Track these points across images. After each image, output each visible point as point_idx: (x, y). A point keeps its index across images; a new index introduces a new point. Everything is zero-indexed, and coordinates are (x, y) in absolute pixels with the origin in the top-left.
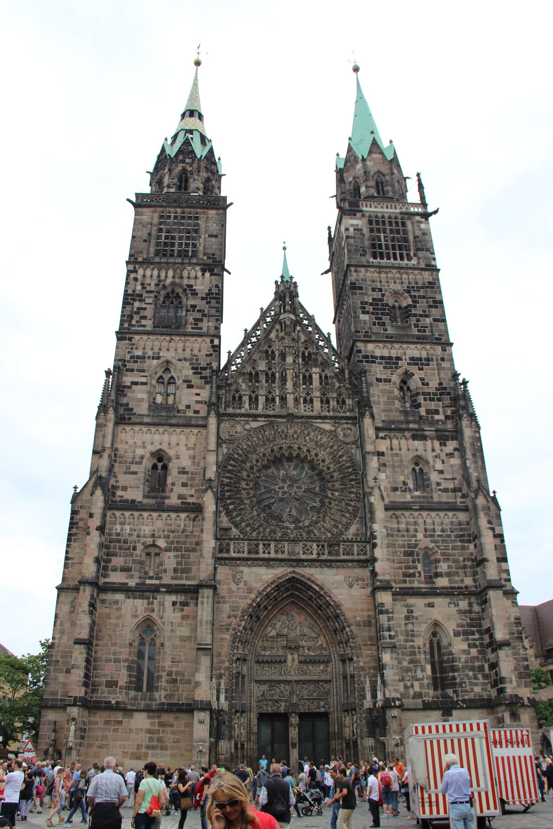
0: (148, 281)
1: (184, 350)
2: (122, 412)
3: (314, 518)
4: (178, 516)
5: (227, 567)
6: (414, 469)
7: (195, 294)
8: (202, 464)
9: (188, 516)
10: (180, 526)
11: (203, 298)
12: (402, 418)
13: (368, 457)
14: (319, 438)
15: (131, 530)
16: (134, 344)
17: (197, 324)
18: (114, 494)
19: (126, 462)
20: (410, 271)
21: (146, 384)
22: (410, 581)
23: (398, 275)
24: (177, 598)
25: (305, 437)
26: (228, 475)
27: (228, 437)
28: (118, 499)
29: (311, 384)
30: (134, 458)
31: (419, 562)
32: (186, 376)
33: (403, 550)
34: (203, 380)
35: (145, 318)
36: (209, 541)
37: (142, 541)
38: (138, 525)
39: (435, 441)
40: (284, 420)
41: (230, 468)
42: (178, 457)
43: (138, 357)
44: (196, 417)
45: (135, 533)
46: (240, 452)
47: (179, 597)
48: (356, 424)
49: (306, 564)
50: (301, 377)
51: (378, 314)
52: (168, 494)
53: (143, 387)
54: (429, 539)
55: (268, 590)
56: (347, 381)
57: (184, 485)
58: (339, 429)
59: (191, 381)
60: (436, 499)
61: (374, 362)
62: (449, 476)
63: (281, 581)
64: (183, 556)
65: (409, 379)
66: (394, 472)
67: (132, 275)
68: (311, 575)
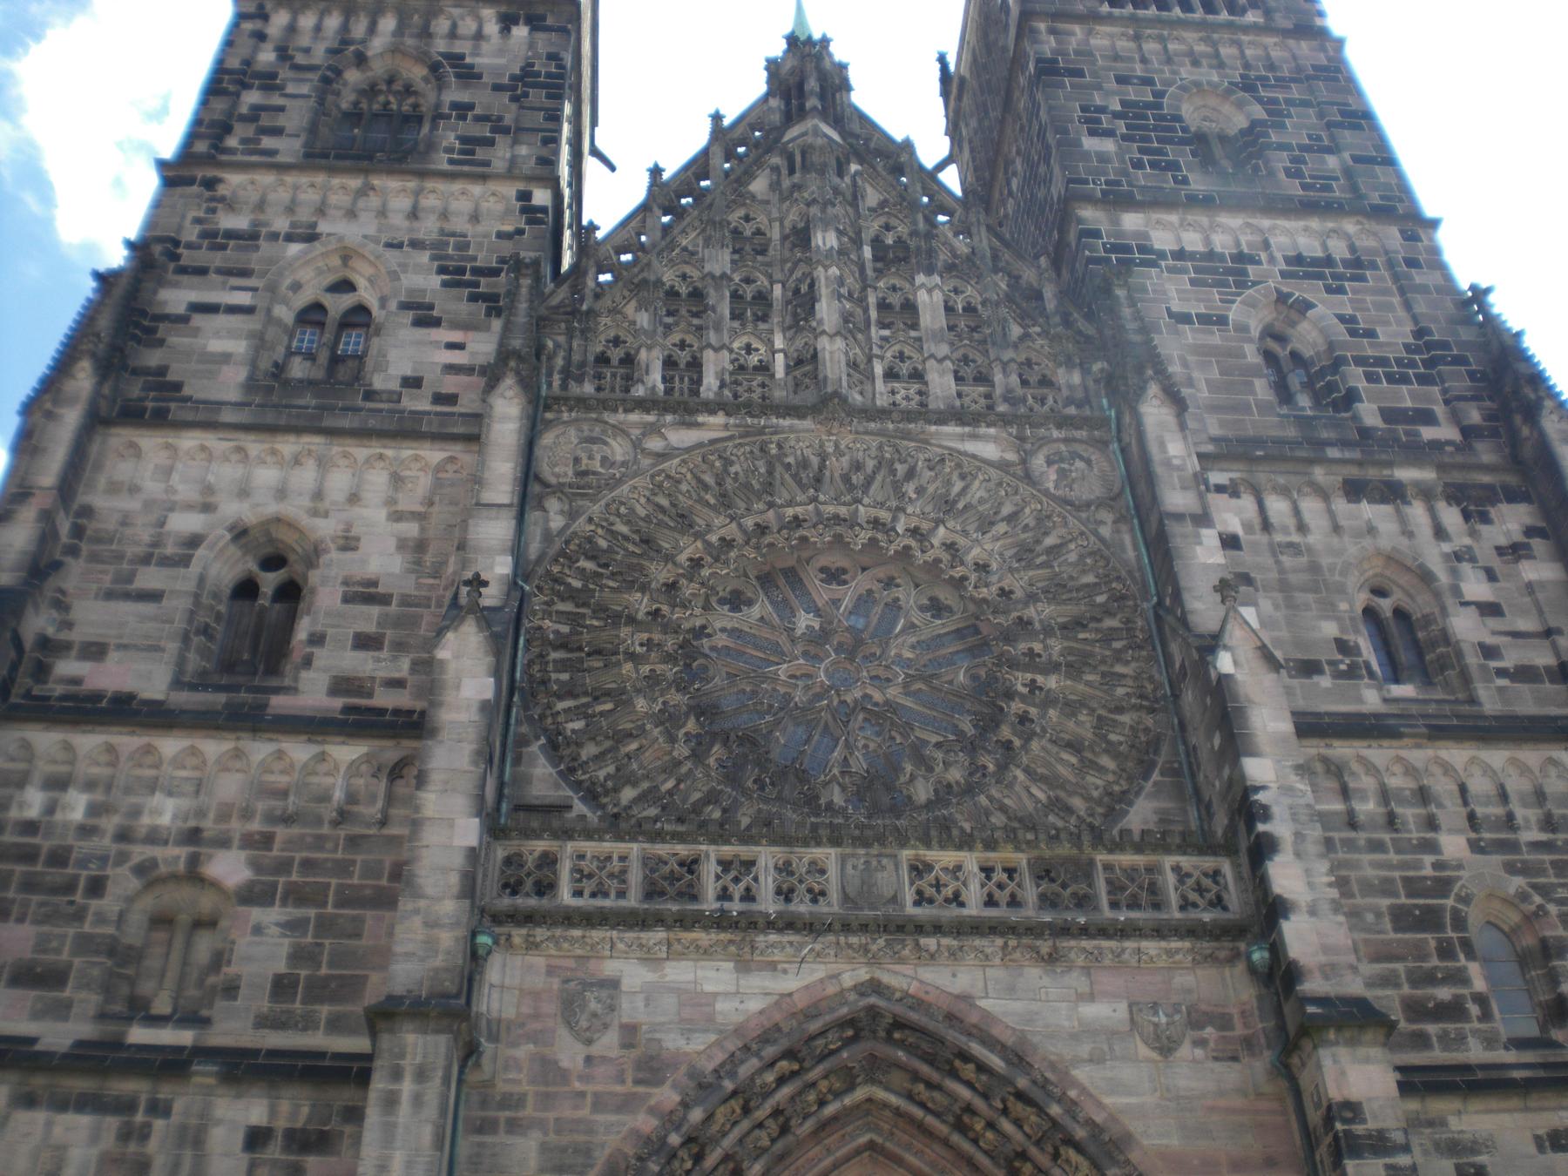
0: (304, 41)
1: (414, 214)
2: (135, 390)
3: (955, 775)
4: (322, 757)
5: (539, 961)
6: (1370, 613)
7: (469, 75)
8: (450, 569)
9: (368, 758)
10: (325, 798)
11: (497, 88)
12: (1291, 432)
13: (1174, 528)
14: (958, 486)
15: (94, 810)
16: (222, 199)
17: (473, 153)
18: (42, 671)
19: (119, 557)
20: (1245, 38)
21: (248, 310)
22: (1444, 1037)
23: (1200, 48)
24: (273, 1112)
25: (897, 487)
26: (568, 607)
27: (570, 477)
28: (59, 690)
29: (915, 326)
30: (155, 545)
31: (1471, 954)
32: (410, 292)
33: (1385, 903)
34: (482, 306)
35: (277, 132)
36: (451, 824)
37: (136, 859)
38: (128, 791)
39: (1441, 506)
40: (808, 423)
41: (577, 584)
42: (349, 543)
43: (231, 235)
44: (437, 414)
45: (110, 823)
46: (623, 529)
47: (285, 1106)
48: (1106, 443)
49: (930, 943)
50: (872, 299)
51: (1149, 140)
52: (287, 682)
53: (235, 321)
54: (1497, 859)
55: (744, 1071)
56: (1057, 319)
57: (364, 642)
58: (1038, 462)
59: (431, 307)
60: (1489, 700)
61: (1153, 264)
62: (1526, 624)
63: (814, 1026)
64: (325, 926)
65: (1293, 324)
66: (1290, 604)
67: (248, 26)
68: (966, 998)
